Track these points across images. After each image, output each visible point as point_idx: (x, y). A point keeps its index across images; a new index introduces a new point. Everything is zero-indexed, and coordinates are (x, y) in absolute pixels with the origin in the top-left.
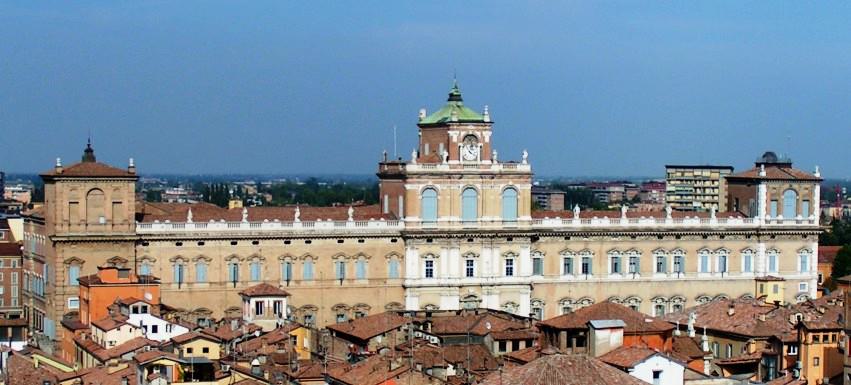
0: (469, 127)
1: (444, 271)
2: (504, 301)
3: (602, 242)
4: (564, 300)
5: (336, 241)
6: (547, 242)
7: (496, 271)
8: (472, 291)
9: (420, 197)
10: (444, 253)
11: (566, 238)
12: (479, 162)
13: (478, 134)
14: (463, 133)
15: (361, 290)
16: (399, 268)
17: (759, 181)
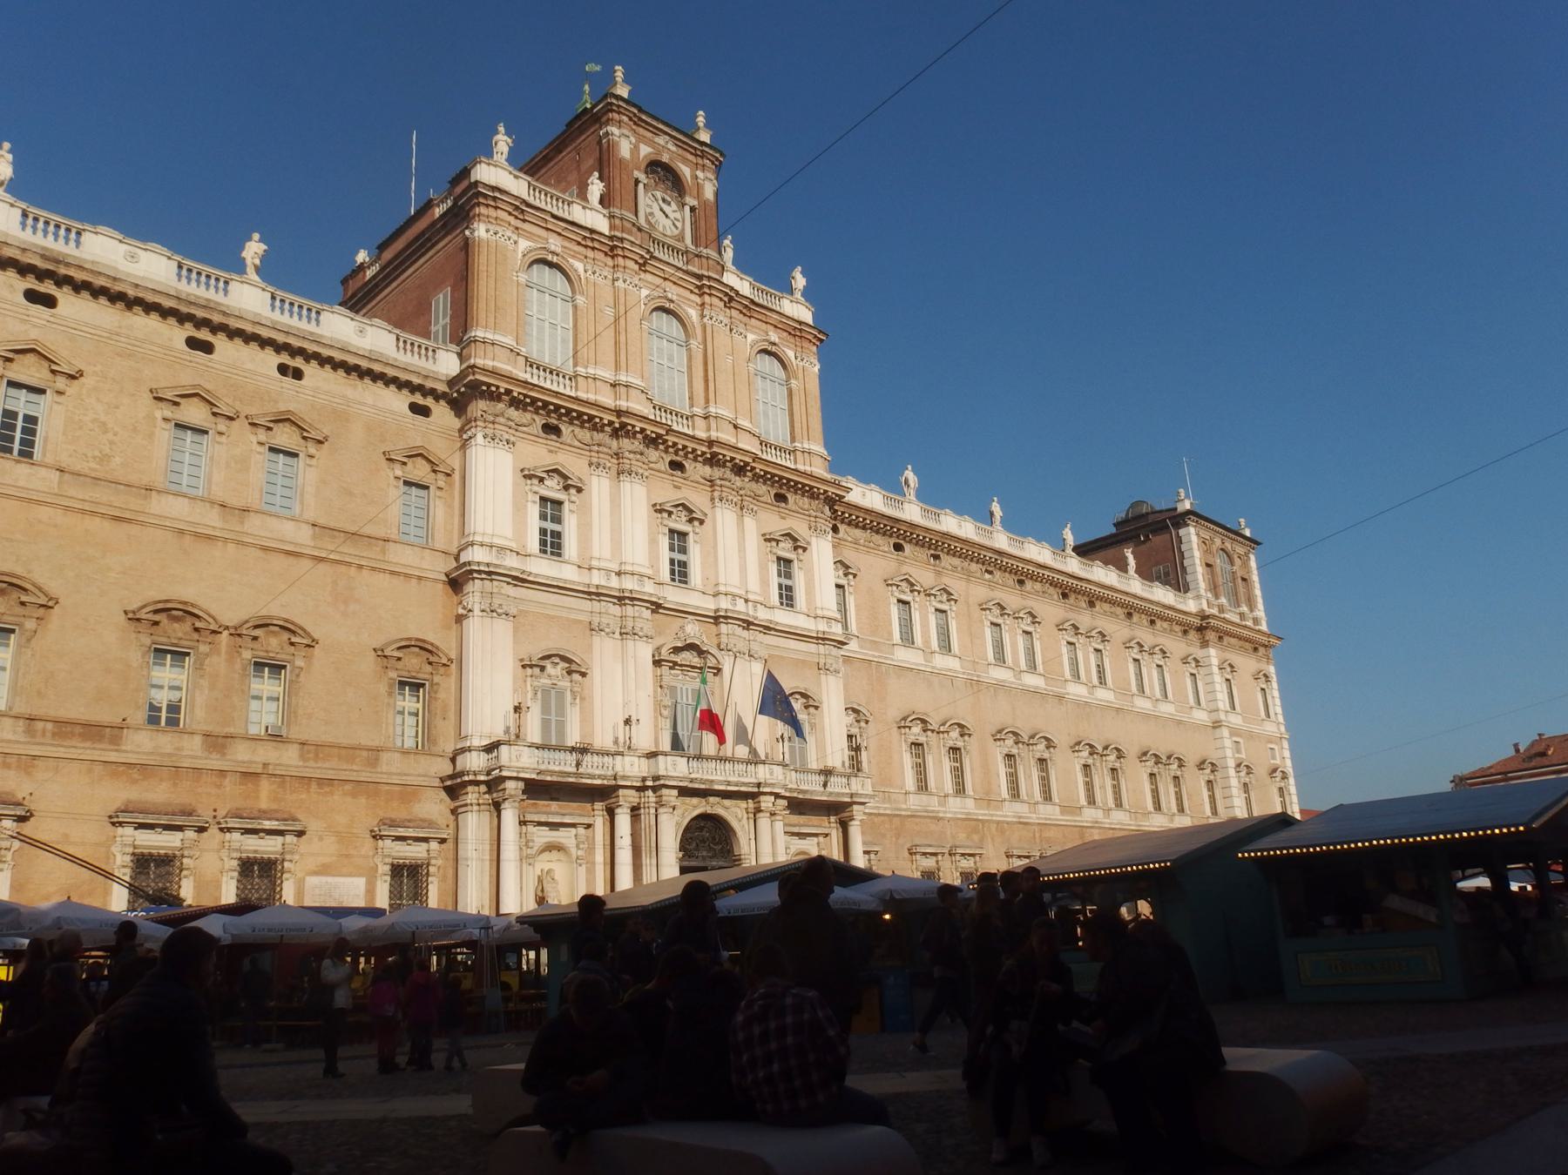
0: (661, 140)
5: (177, 335)
7: (754, 584)
8: (693, 631)
10: (599, 486)
11: (898, 548)
13: (685, 171)
14: (645, 150)
15: (279, 562)
17: (1180, 520)
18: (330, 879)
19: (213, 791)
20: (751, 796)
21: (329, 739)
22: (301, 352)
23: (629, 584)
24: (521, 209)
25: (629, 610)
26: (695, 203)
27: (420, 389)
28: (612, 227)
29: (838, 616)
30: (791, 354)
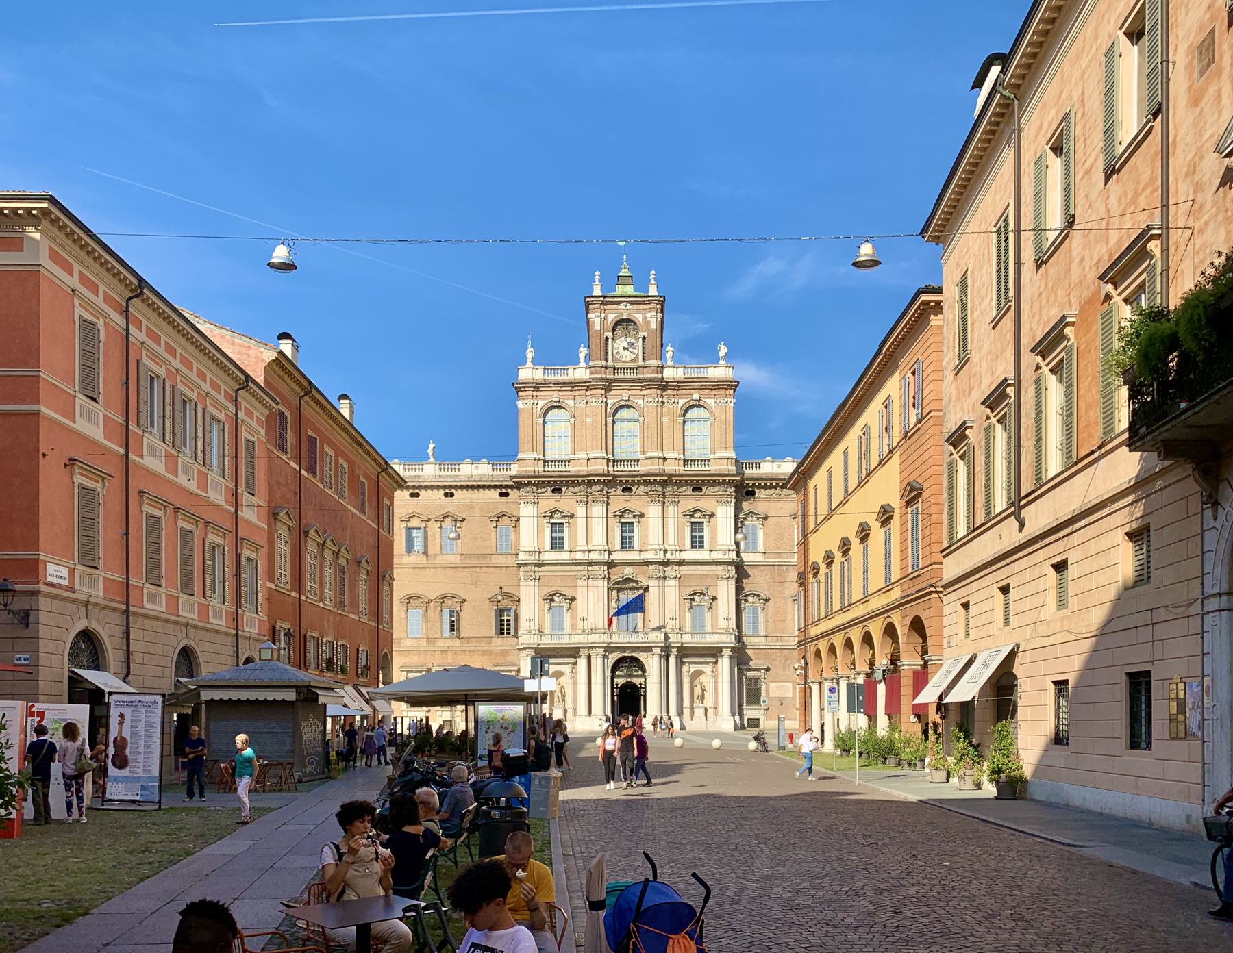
0: (622, 306)
1: (581, 540)
2: (689, 591)
6: (769, 498)
9: (541, 421)
10: (581, 511)
12: (641, 363)
13: (638, 317)
14: (612, 317)
15: (449, 572)
16: (513, 536)
20: (648, 649)
22: (450, 487)
23: (594, 556)
24: (537, 386)
25: (595, 567)
26: (645, 334)
27: (500, 487)
28: (591, 373)
29: (734, 547)
30: (711, 402)
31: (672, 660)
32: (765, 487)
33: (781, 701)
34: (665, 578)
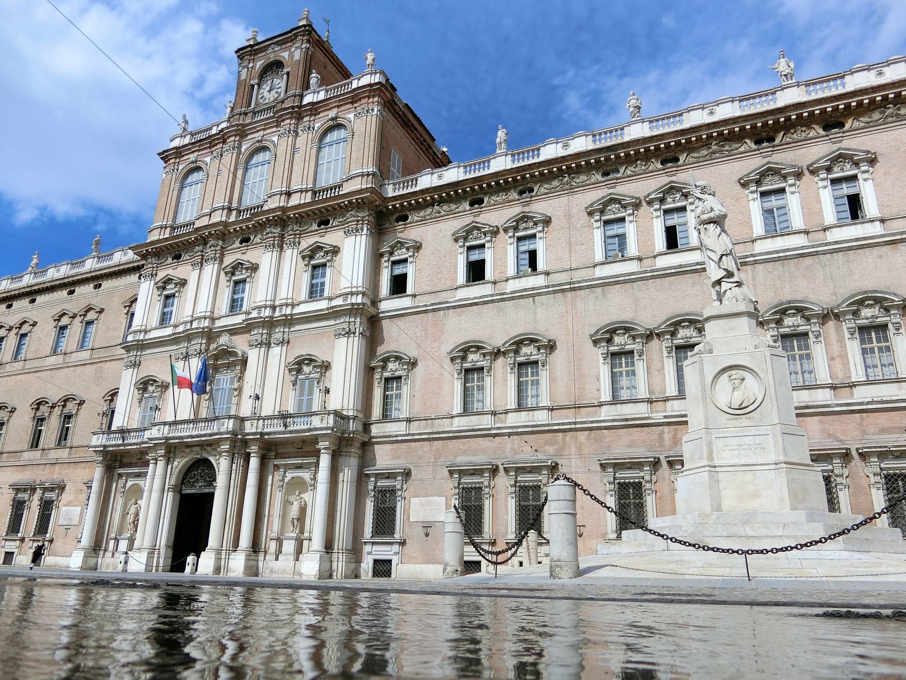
3: (571, 190)
4: (465, 350)
9: (177, 185)
13: (285, 55)
14: (259, 64)
18: (69, 508)
19: (42, 472)
21: (81, 444)
26: (289, 69)
31: (254, 462)
32: (419, 207)
33: (427, 528)
34: (269, 345)
